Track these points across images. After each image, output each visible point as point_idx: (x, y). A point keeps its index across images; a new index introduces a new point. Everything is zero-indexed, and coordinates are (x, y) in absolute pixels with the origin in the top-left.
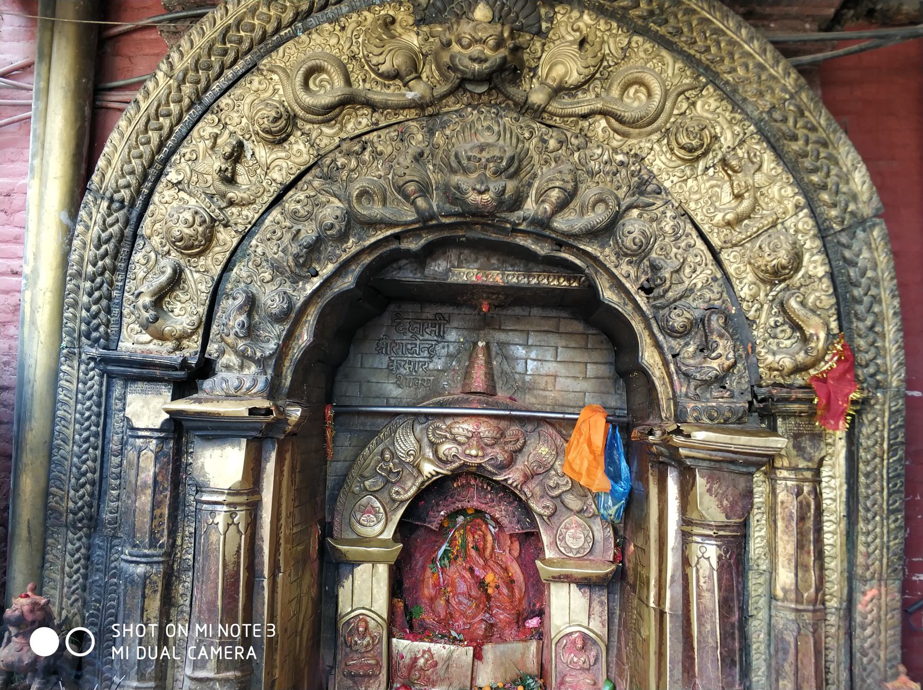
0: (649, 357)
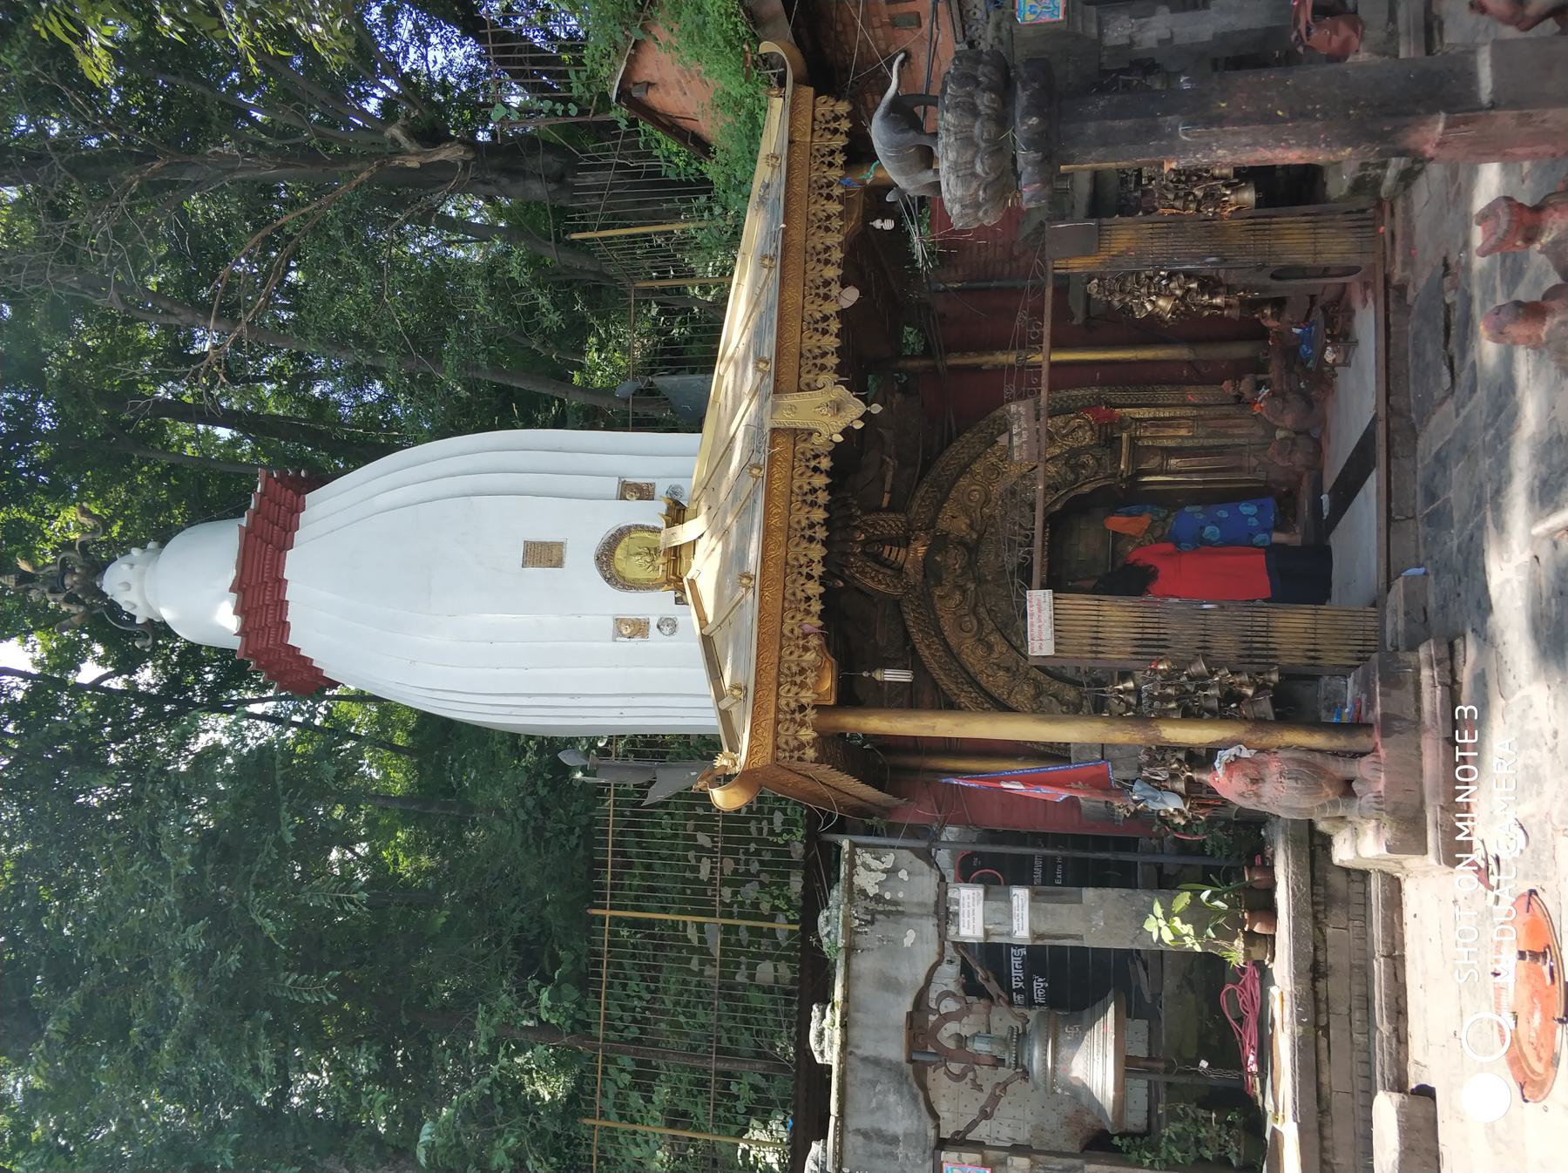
0: (1086, 489)
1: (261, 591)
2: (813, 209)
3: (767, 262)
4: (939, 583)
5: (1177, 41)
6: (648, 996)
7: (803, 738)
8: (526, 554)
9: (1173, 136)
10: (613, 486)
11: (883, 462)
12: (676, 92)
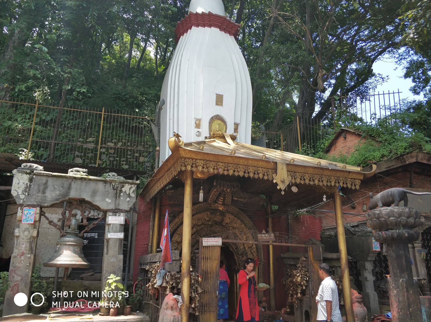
0: (236, 258)
1: (207, 20)
2: (333, 178)
3: (319, 164)
4: (211, 214)
5: (366, 282)
6: (69, 125)
7: (188, 167)
8: (220, 95)
9: (401, 277)
10: (238, 122)
11: (246, 198)
12: (343, 145)
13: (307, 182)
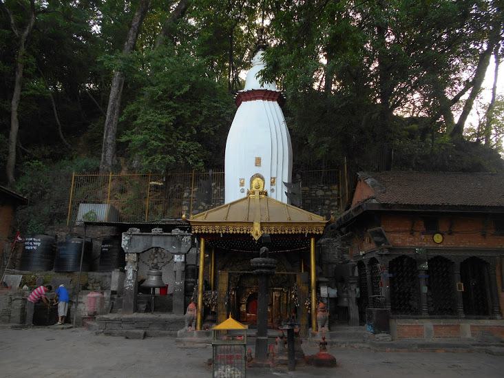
10: (274, 176)
13: (280, 232)
